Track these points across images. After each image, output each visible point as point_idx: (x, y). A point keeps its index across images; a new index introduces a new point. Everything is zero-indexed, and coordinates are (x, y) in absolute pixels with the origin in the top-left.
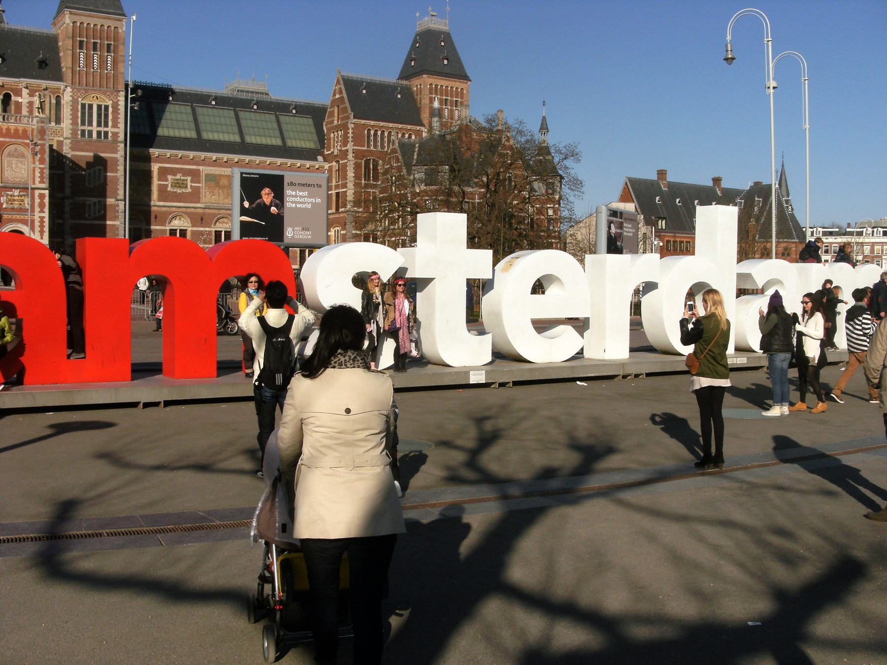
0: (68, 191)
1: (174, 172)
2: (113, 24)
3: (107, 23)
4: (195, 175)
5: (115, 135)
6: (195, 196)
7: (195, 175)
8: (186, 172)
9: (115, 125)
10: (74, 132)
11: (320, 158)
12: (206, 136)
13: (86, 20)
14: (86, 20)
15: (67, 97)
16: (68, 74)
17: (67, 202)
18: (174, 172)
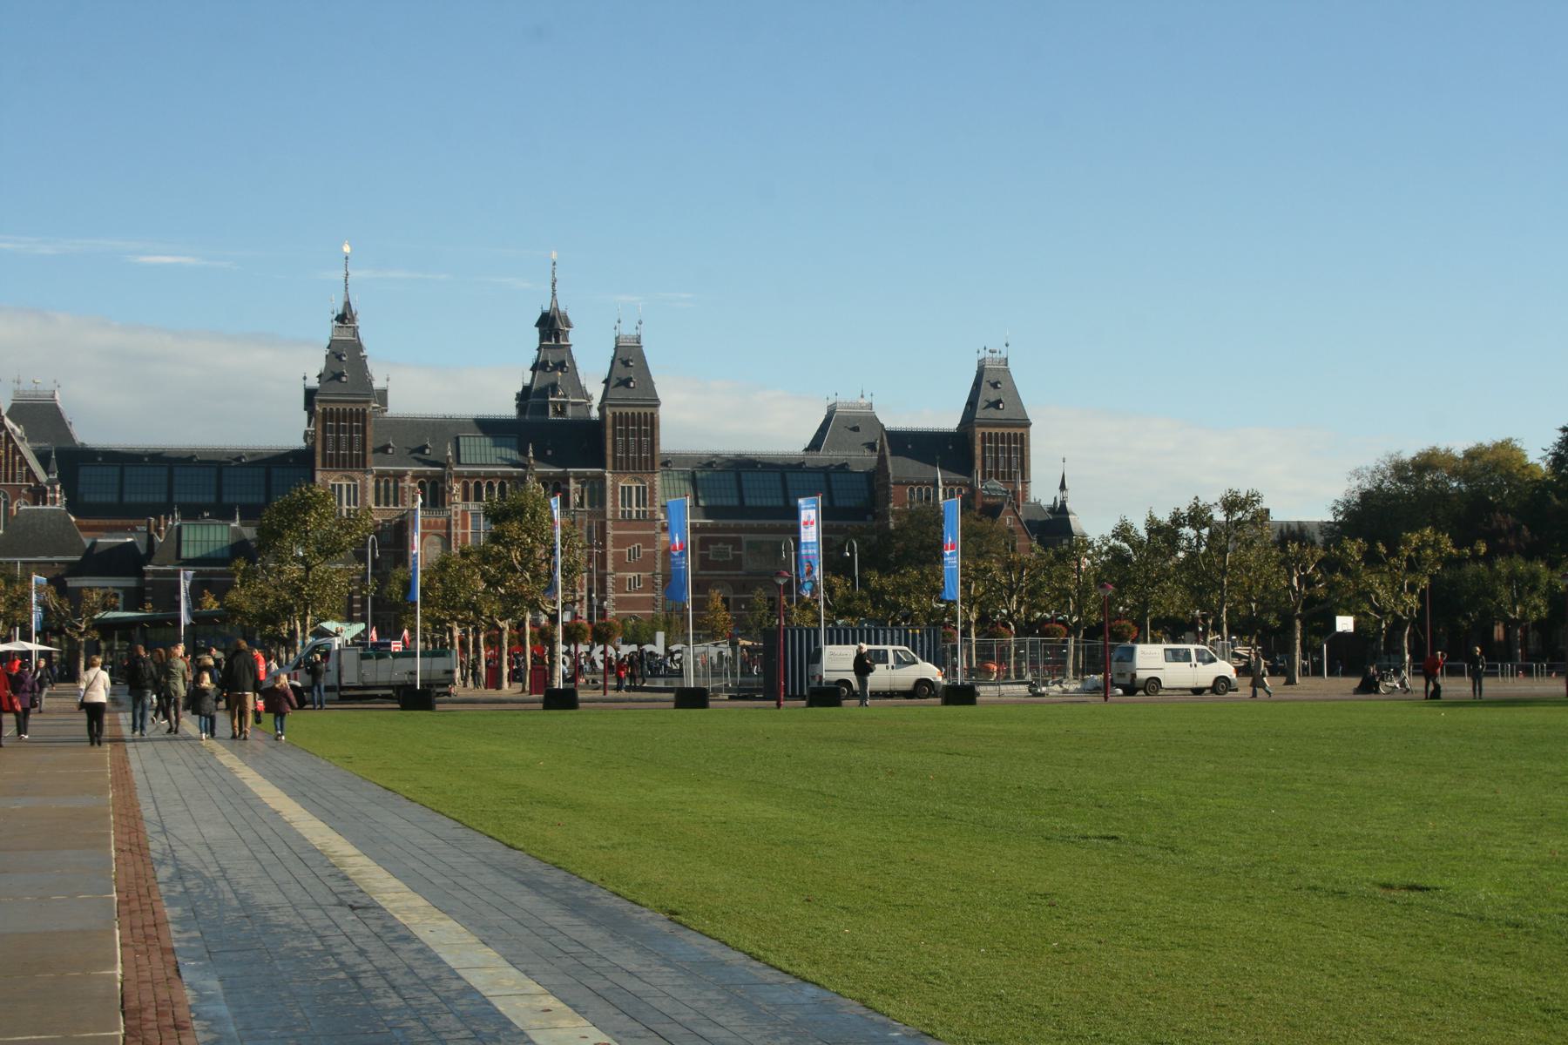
0: (610, 568)
1: (716, 541)
2: (649, 410)
3: (642, 410)
4: (737, 543)
5: (653, 513)
6: (737, 563)
7: (737, 543)
8: (726, 541)
9: (652, 505)
10: (615, 513)
11: (869, 517)
12: (748, 502)
13: (624, 410)
14: (624, 410)
15: (609, 483)
16: (609, 461)
17: (610, 579)
18: (716, 541)
